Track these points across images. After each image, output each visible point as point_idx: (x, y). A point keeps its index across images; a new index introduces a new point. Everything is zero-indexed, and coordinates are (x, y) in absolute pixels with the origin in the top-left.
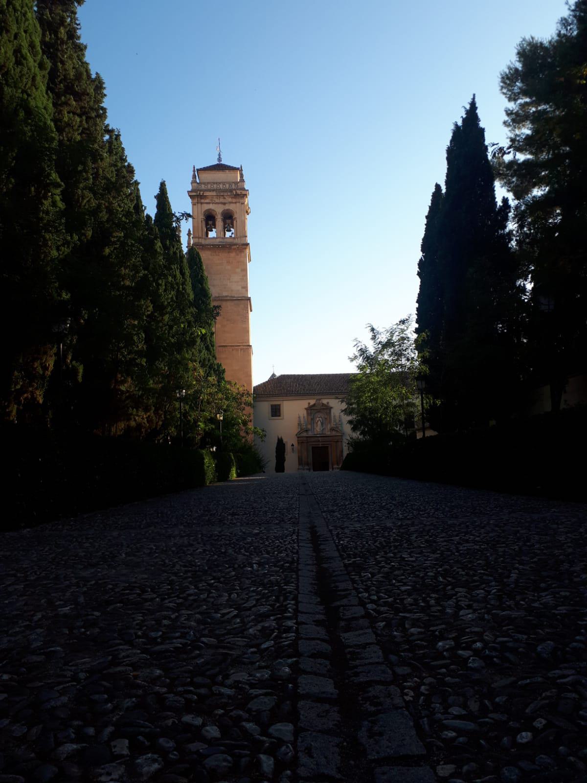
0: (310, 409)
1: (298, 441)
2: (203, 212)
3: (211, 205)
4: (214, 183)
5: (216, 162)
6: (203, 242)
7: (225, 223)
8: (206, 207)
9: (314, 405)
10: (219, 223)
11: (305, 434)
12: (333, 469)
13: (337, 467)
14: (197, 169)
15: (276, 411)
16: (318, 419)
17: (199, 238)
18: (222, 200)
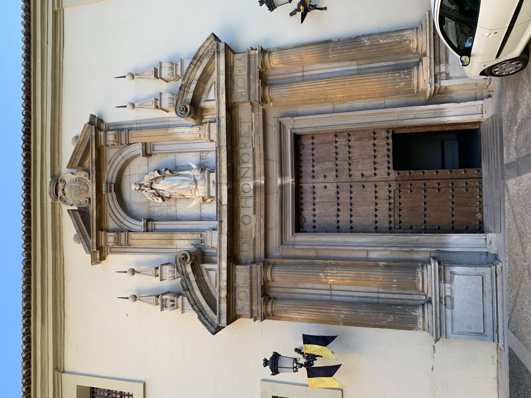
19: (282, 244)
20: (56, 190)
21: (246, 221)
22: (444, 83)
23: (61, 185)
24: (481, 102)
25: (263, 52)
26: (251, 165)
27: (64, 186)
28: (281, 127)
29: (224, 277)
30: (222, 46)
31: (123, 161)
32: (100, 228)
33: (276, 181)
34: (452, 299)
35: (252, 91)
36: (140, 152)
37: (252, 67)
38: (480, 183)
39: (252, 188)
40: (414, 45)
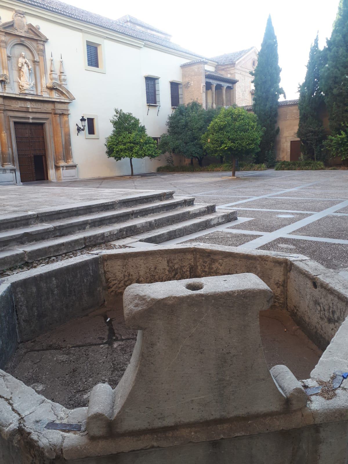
9: (11, 25)
12: (57, 168)
13: (66, 164)
19: (10, 117)
20: (20, 13)
21: (16, 103)
22: (61, 169)
23: (22, 16)
24: (55, 178)
26: (35, 107)
27: (21, 17)
30: (71, 101)
31: (32, 50)
33: (31, 116)
34: (5, 173)
35: (58, 110)
36: (36, 60)
37: (65, 111)
38: (32, 181)
39: (28, 106)
40: (70, 161)
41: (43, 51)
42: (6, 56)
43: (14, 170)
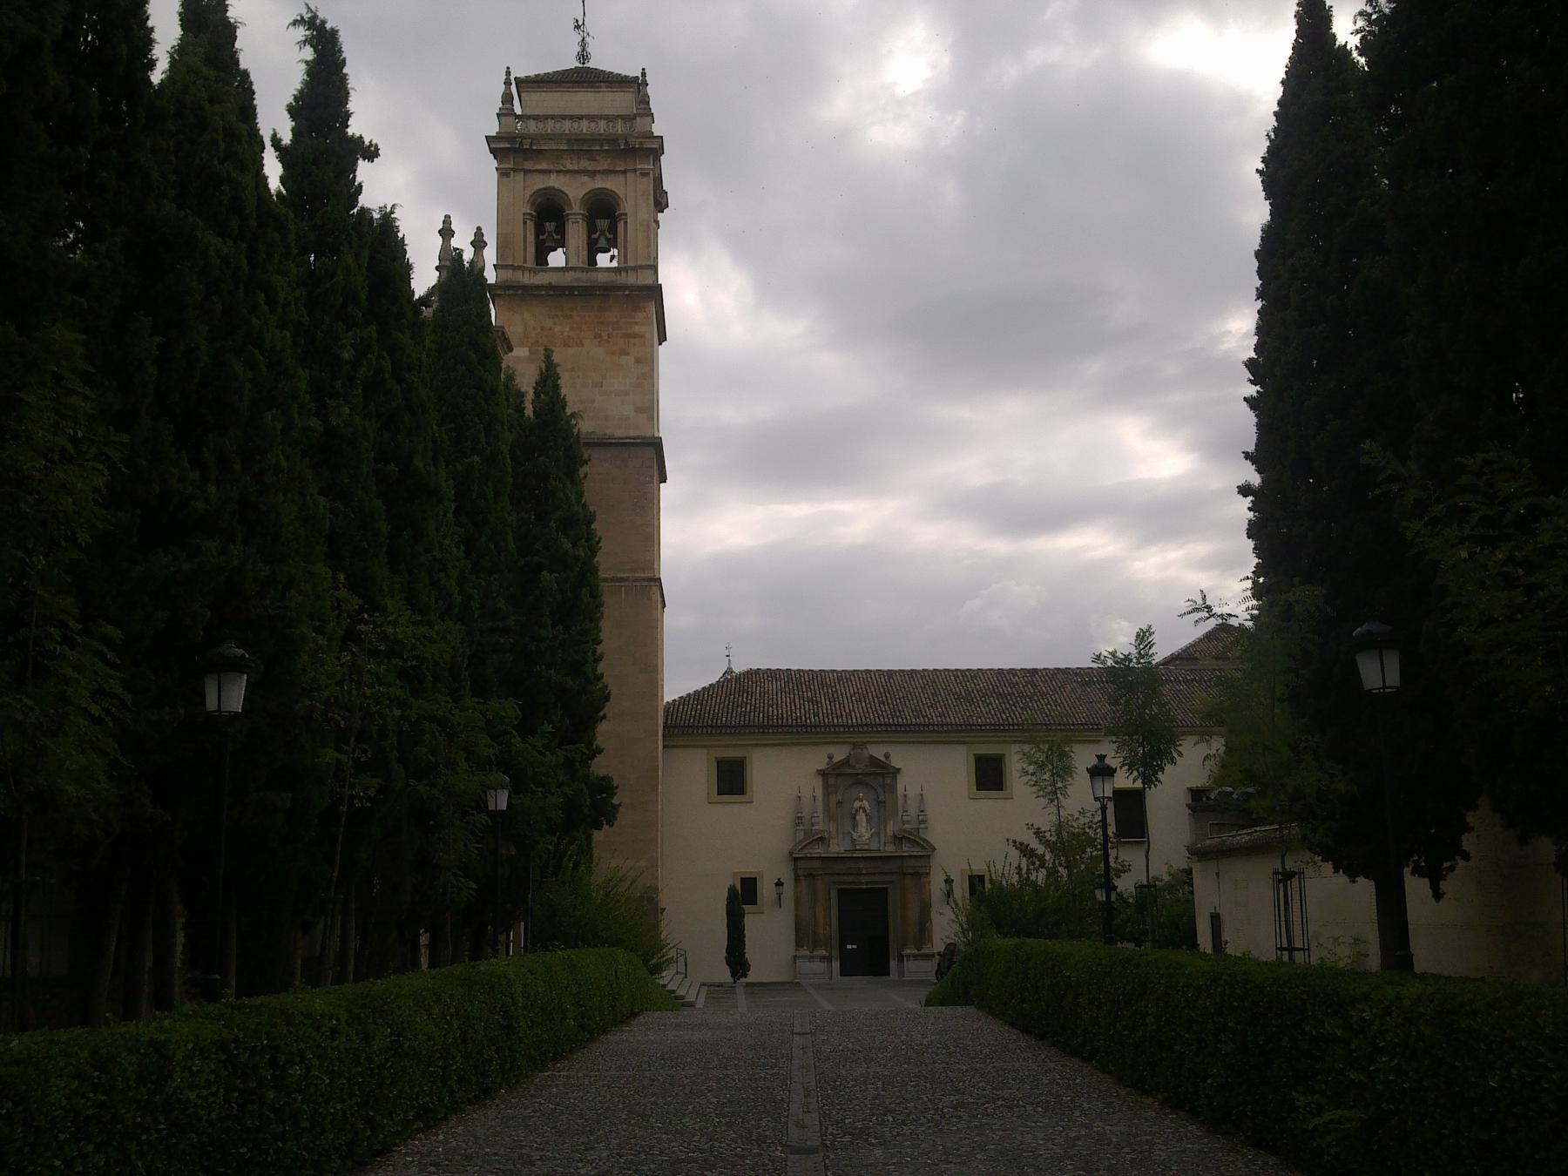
0: (832, 775)
1: (795, 870)
2: (527, 196)
3: (553, 176)
4: (564, 117)
5: (573, 63)
6: (527, 279)
7: (592, 228)
8: (539, 182)
10: (576, 233)
11: (818, 851)
12: (901, 958)
13: (915, 952)
14: (515, 78)
15: (731, 780)
16: (857, 804)
17: (514, 268)
18: (586, 164)
25: (928, 874)
28: (891, 882)
29: (818, 855)
32: (838, 775)
41: (893, 786)
42: (835, 803)
43: (828, 959)
